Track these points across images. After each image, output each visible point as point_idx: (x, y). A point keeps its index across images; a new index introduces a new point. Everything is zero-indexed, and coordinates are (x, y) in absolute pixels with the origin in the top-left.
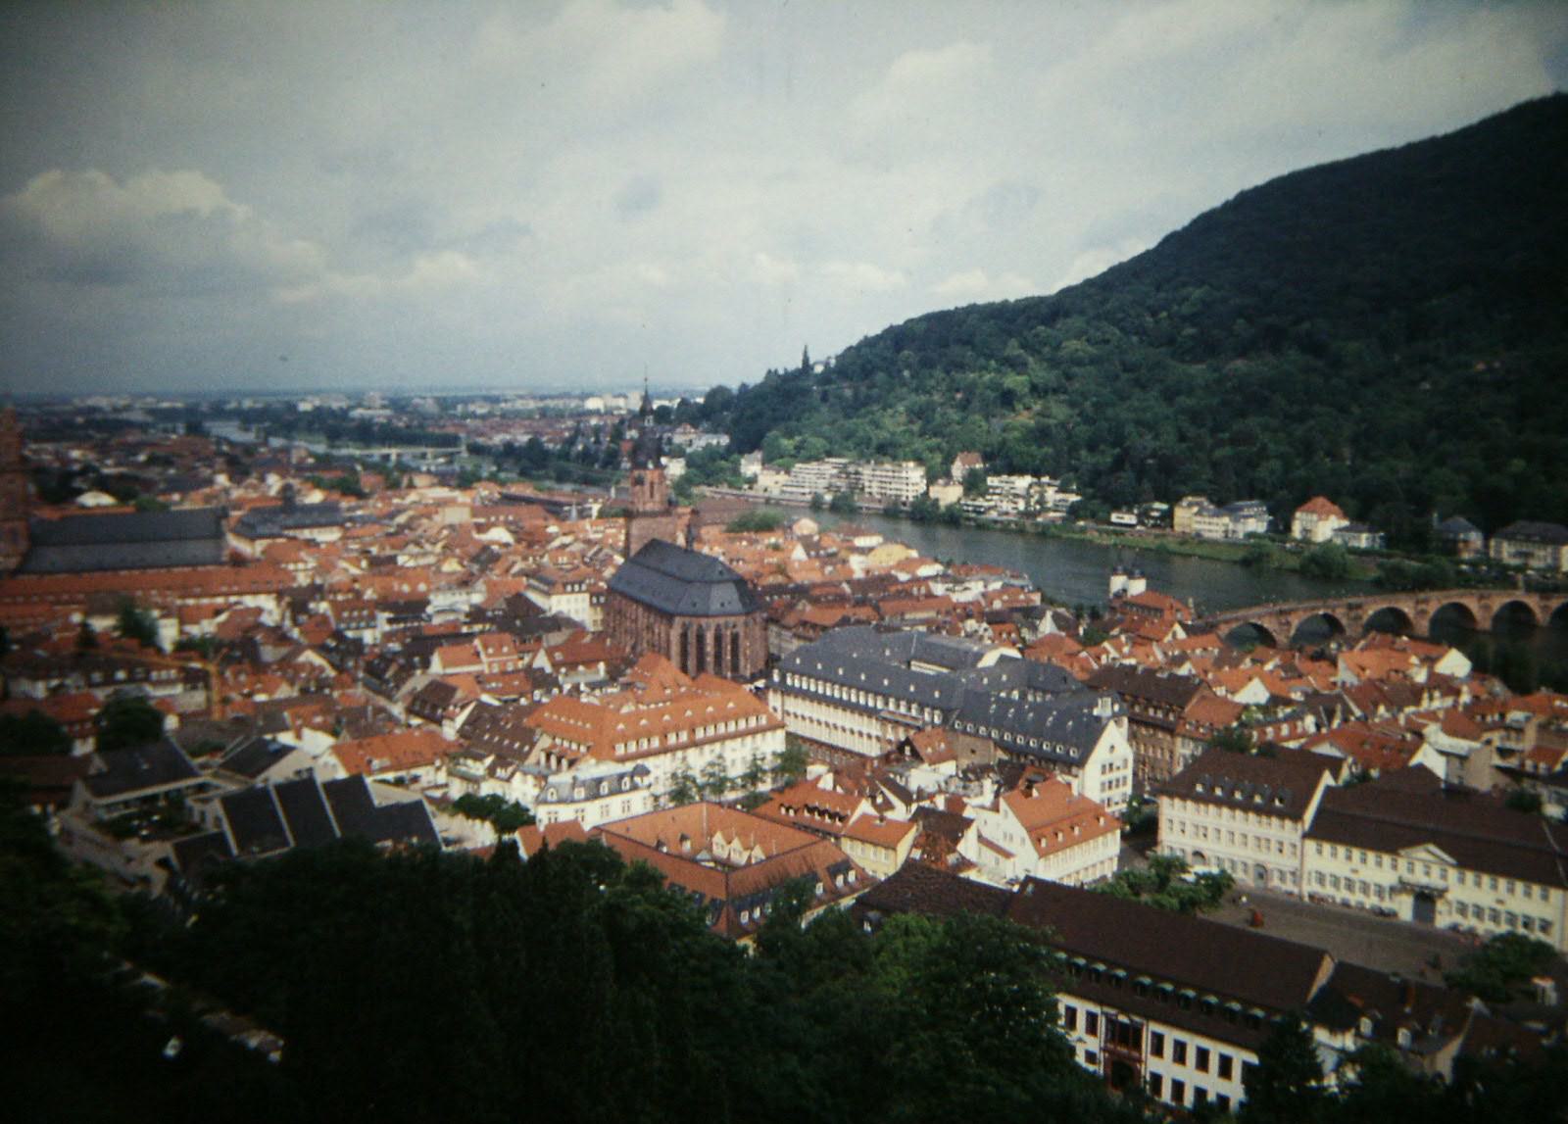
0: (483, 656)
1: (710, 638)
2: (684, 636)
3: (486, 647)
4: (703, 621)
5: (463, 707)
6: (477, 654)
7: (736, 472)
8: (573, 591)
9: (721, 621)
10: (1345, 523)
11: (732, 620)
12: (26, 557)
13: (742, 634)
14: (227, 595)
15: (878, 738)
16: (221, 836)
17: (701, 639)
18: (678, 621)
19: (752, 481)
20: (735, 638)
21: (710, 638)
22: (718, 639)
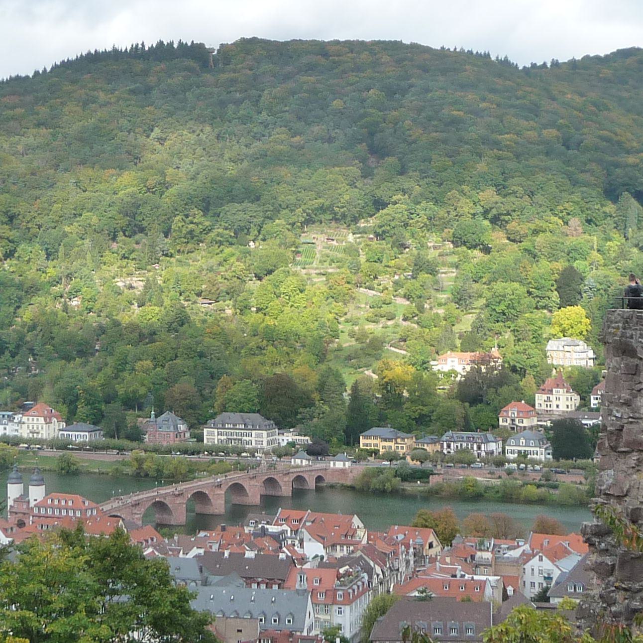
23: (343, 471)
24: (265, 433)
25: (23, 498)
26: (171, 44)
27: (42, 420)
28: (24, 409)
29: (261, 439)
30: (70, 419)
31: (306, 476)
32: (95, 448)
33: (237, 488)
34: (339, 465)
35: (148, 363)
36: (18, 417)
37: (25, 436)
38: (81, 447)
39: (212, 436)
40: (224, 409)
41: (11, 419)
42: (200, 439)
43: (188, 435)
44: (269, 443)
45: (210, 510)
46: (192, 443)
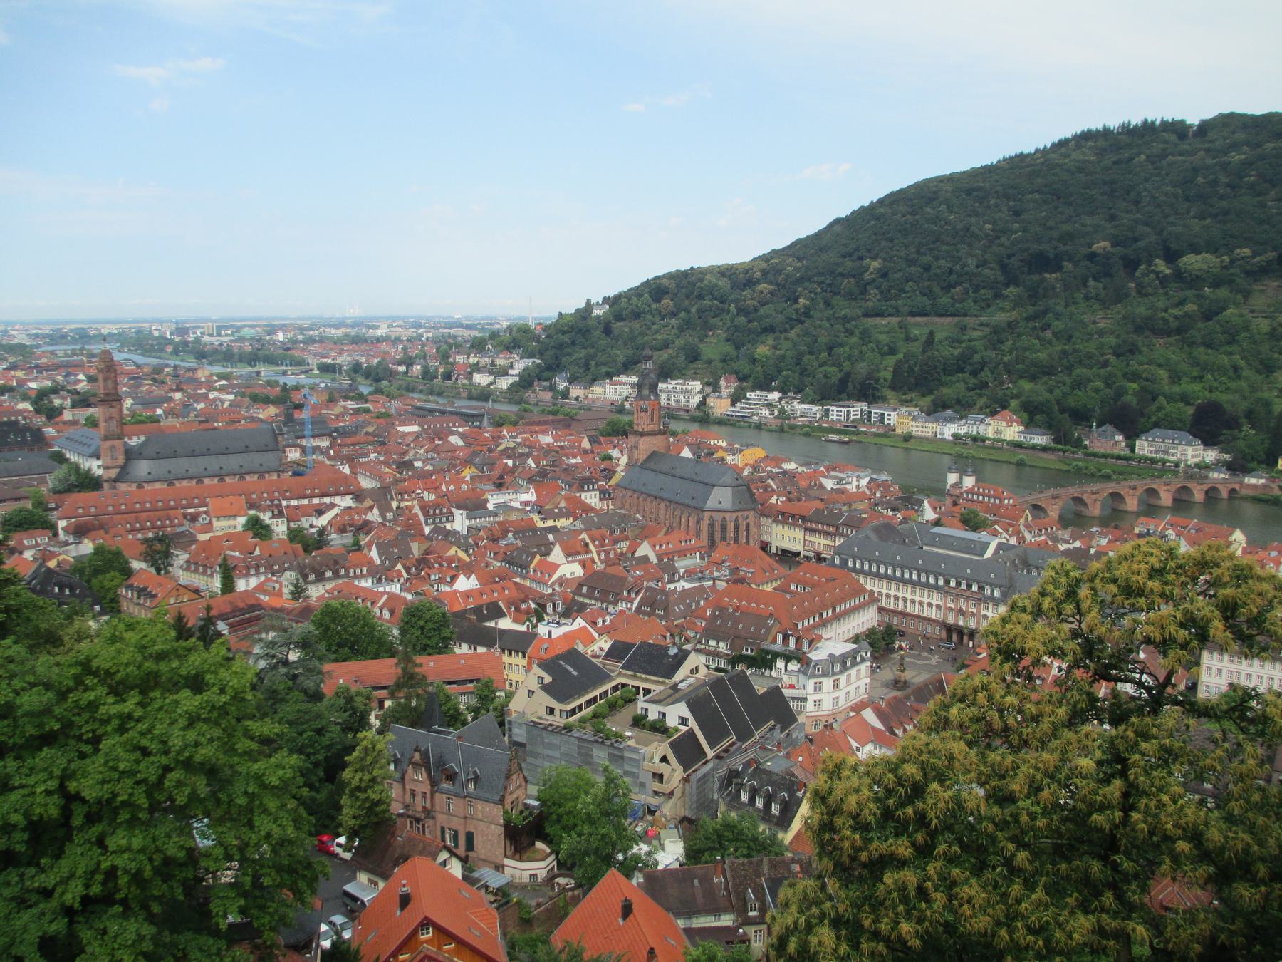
0: (591, 547)
1: (731, 526)
2: (711, 525)
3: (593, 541)
4: (728, 516)
5: (637, 593)
6: (587, 545)
7: (552, 388)
8: (588, 490)
9: (740, 514)
10: (1022, 428)
11: (746, 513)
12: (123, 468)
13: (752, 524)
14: (311, 497)
15: (938, 607)
16: (691, 732)
17: (724, 528)
18: (707, 515)
19: (565, 394)
20: (748, 526)
21: (731, 526)
22: (737, 528)
23: (1255, 486)
24: (1190, 449)
25: (958, 485)
26: (1153, 123)
27: (1004, 424)
28: (993, 414)
29: (1193, 453)
30: (1030, 425)
31: (1220, 487)
32: (1044, 449)
33: (1116, 496)
34: (1253, 481)
35: (1099, 384)
36: (988, 420)
37: (990, 436)
38: (1034, 447)
39: (1144, 447)
40: (1157, 425)
41: (982, 421)
42: (1133, 450)
43: (1123, 444)
44: (1193, 456)
45: (1122, 507)
46: (1127, 453)
